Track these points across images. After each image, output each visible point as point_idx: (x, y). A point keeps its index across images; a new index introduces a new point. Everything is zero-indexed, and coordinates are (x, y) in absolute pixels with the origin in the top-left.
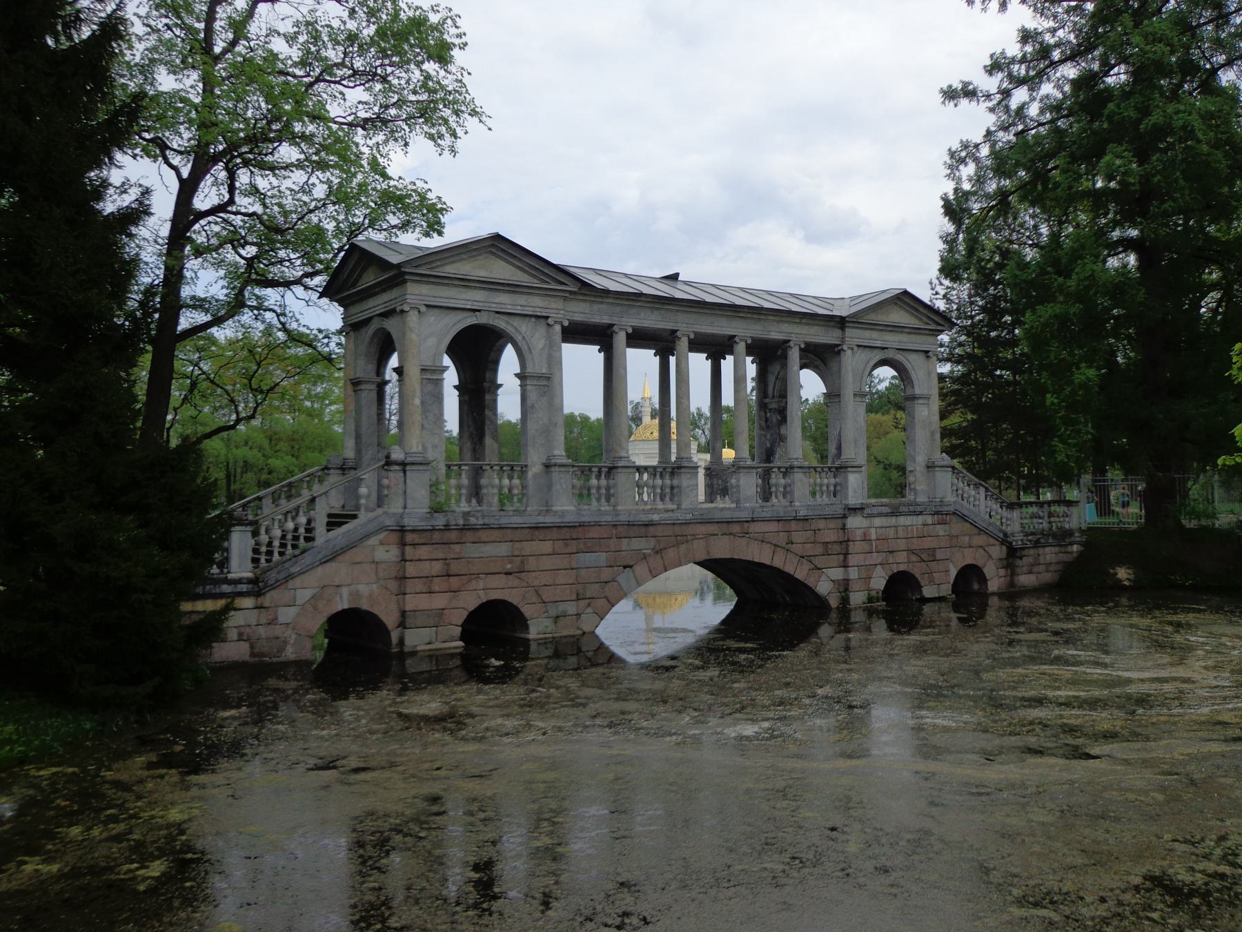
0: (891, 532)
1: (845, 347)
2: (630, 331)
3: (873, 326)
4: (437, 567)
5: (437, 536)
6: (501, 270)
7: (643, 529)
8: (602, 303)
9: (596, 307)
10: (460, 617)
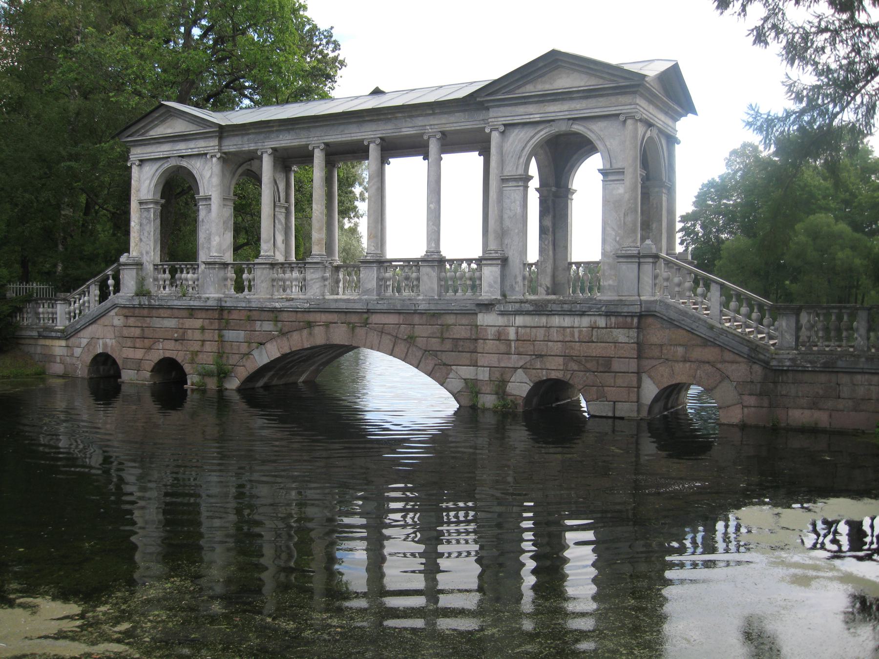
0: (540, 334)
1: (487, 130)
2: (270, 151)
3: (525, 101)
4: (137, 332)
5: (137, 311)
7: (271, 315)
8: (249, 134)
9: (246, 138)
10: (149, 365)
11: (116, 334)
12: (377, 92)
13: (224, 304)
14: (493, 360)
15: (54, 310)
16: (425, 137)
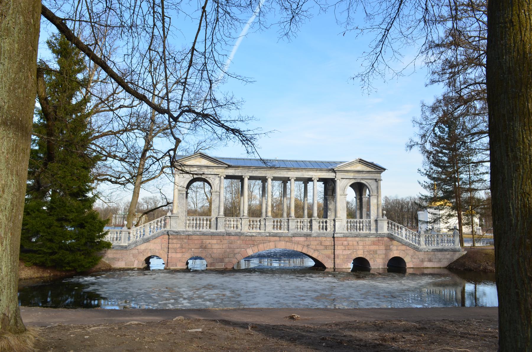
1: (336, 179)
4: (179, 245)
6: (204, 162)
9: (237, 171)
11: (163, 247)
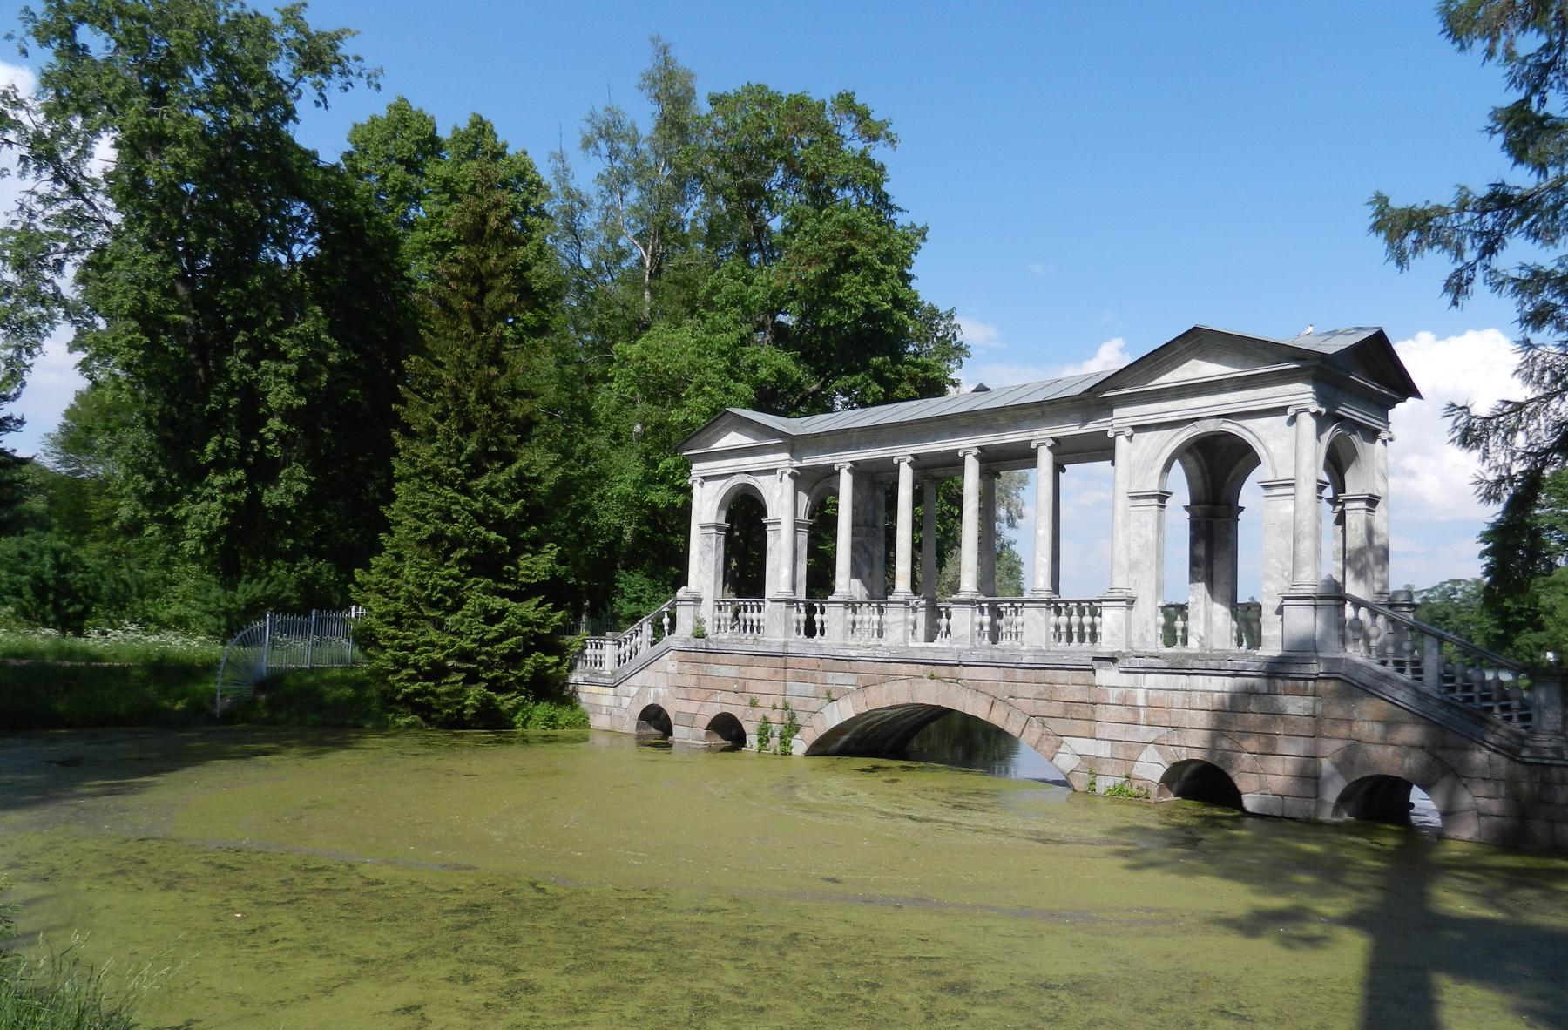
0: (1178, 699)
1: (1110, 435)
4: (692, 681)
12: (982, 389)
13: (791, 650)
14: (1117, 732)
15: (602, 652)
16: (1033, 445)
